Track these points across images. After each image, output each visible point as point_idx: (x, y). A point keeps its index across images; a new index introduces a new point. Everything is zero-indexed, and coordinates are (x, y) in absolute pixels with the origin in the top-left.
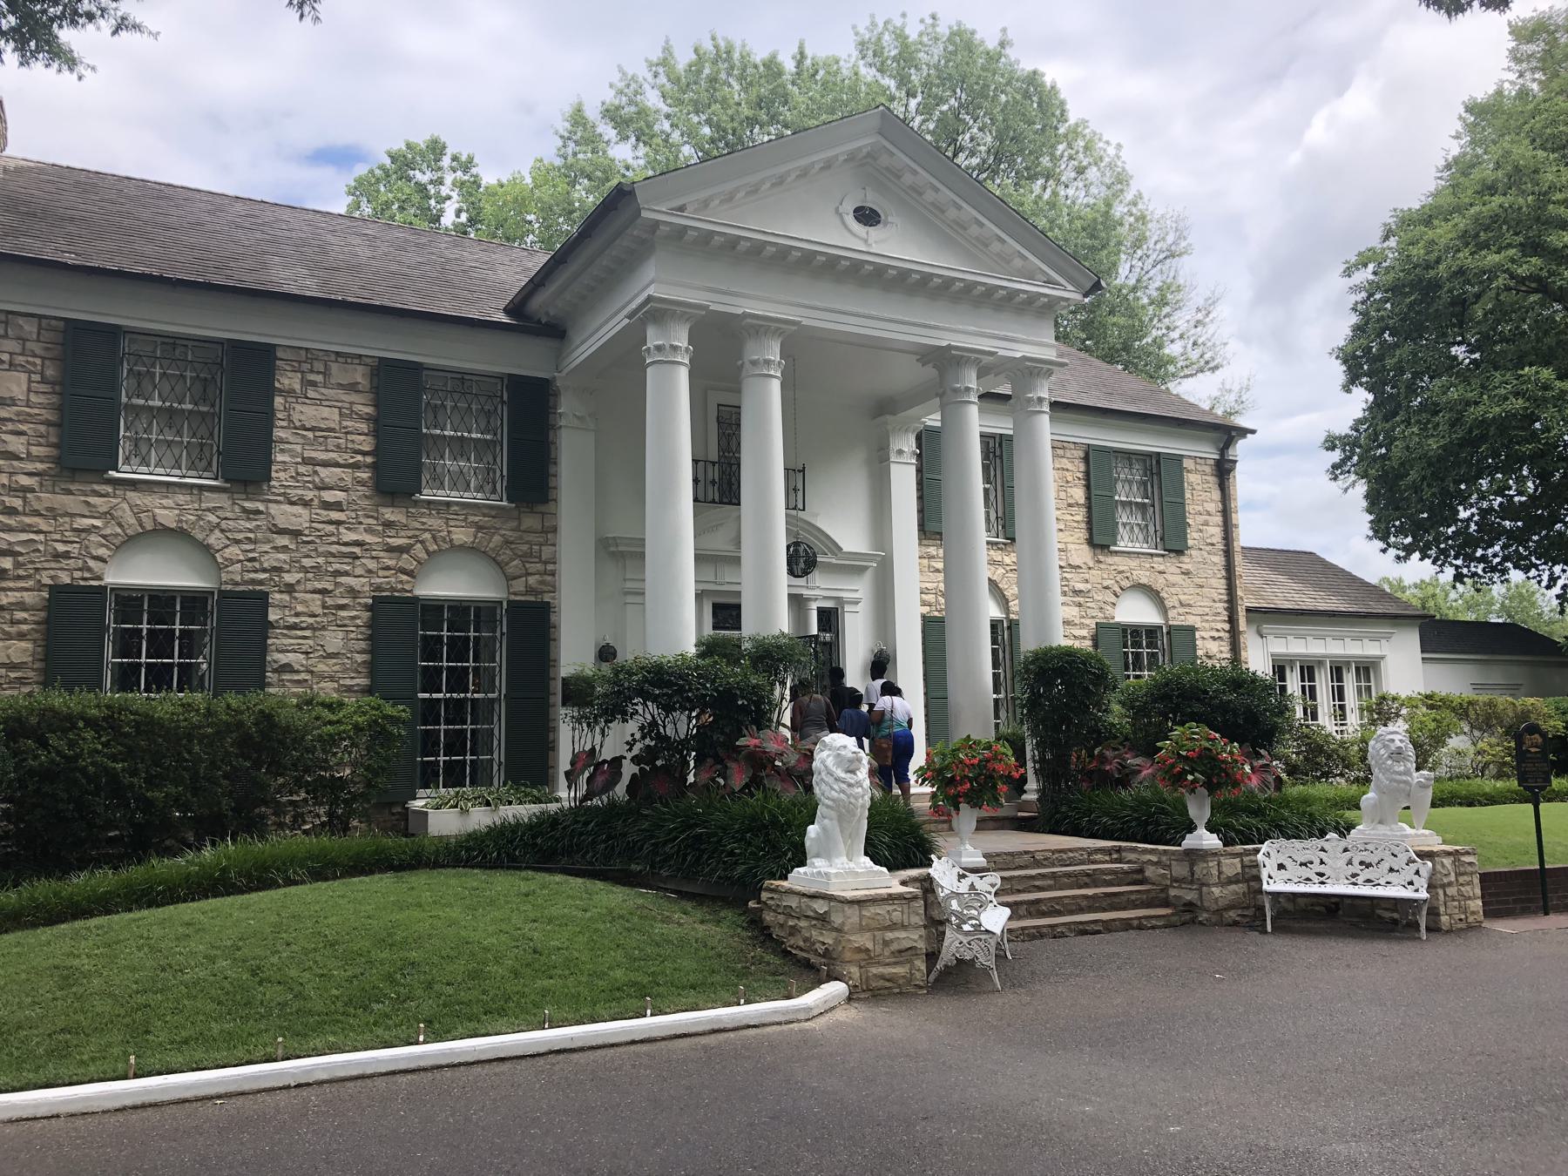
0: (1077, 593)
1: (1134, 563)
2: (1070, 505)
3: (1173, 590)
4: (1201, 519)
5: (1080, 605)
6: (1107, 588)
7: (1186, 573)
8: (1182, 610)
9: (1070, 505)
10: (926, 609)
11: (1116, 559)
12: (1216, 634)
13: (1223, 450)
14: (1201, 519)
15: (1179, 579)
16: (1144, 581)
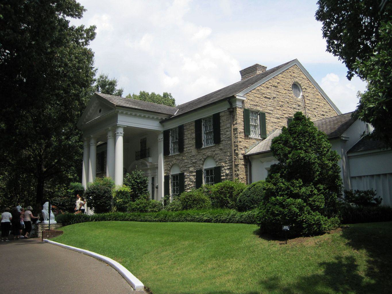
0: (194, 163)
1: (207, 151)
2: (193, 139)
3: (217, 156)
4: (225, 131)
5: (194, 166)
6: (200, 160)
7: (221, 149)
8: (219, 162)
9: (193, 139)
10: (165, 175)
11: (203, 151)
12: (229, 167)
13: (231, 104)
14: (225, 131)
15: (219, 152)
16: (210, 155)
